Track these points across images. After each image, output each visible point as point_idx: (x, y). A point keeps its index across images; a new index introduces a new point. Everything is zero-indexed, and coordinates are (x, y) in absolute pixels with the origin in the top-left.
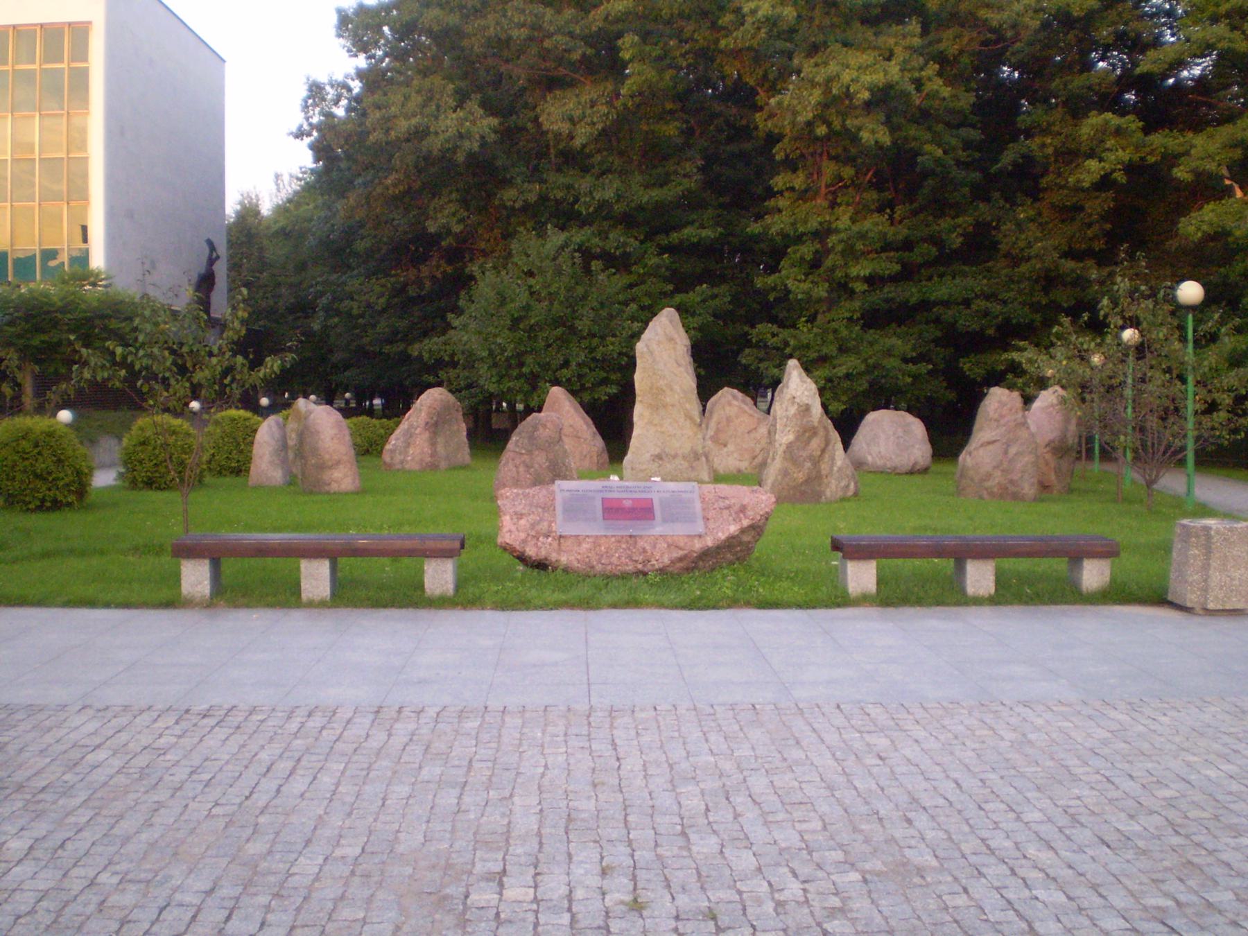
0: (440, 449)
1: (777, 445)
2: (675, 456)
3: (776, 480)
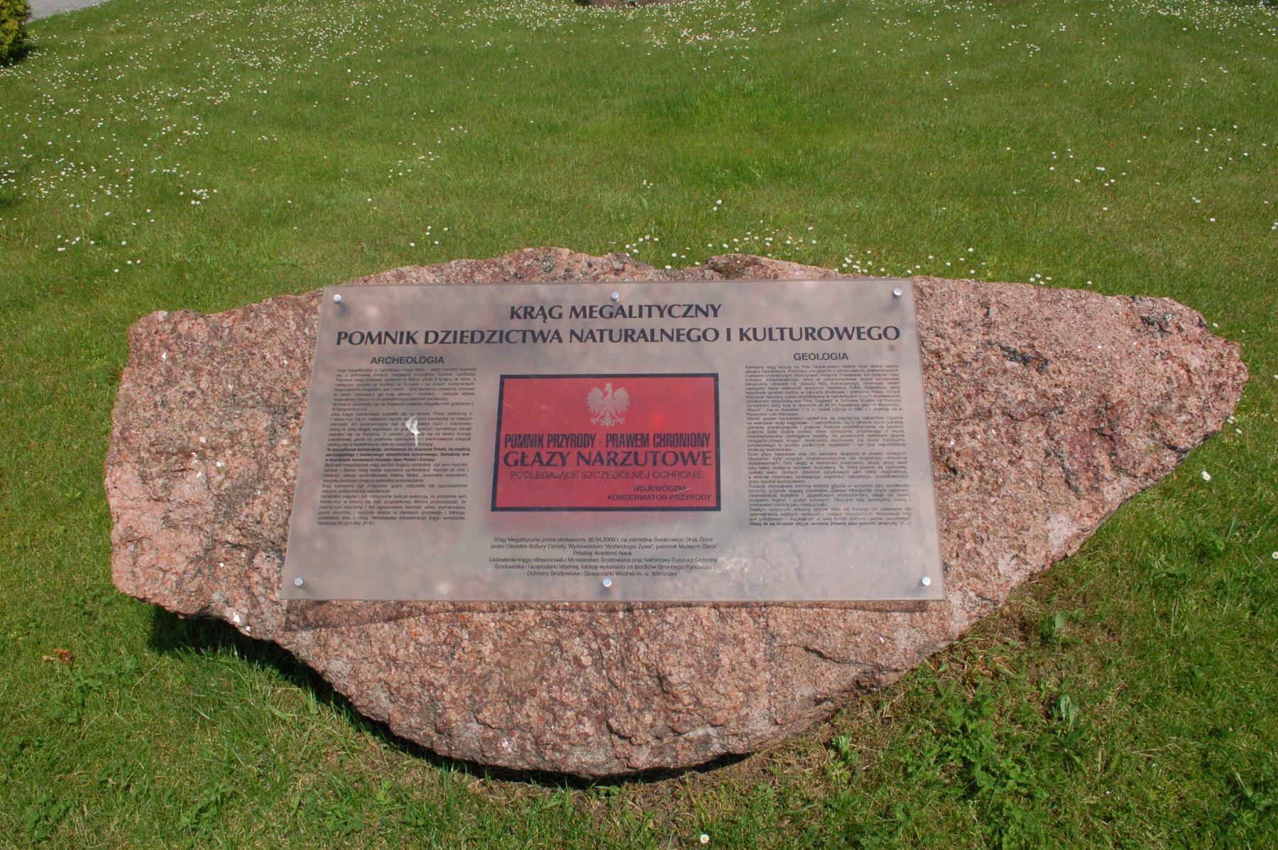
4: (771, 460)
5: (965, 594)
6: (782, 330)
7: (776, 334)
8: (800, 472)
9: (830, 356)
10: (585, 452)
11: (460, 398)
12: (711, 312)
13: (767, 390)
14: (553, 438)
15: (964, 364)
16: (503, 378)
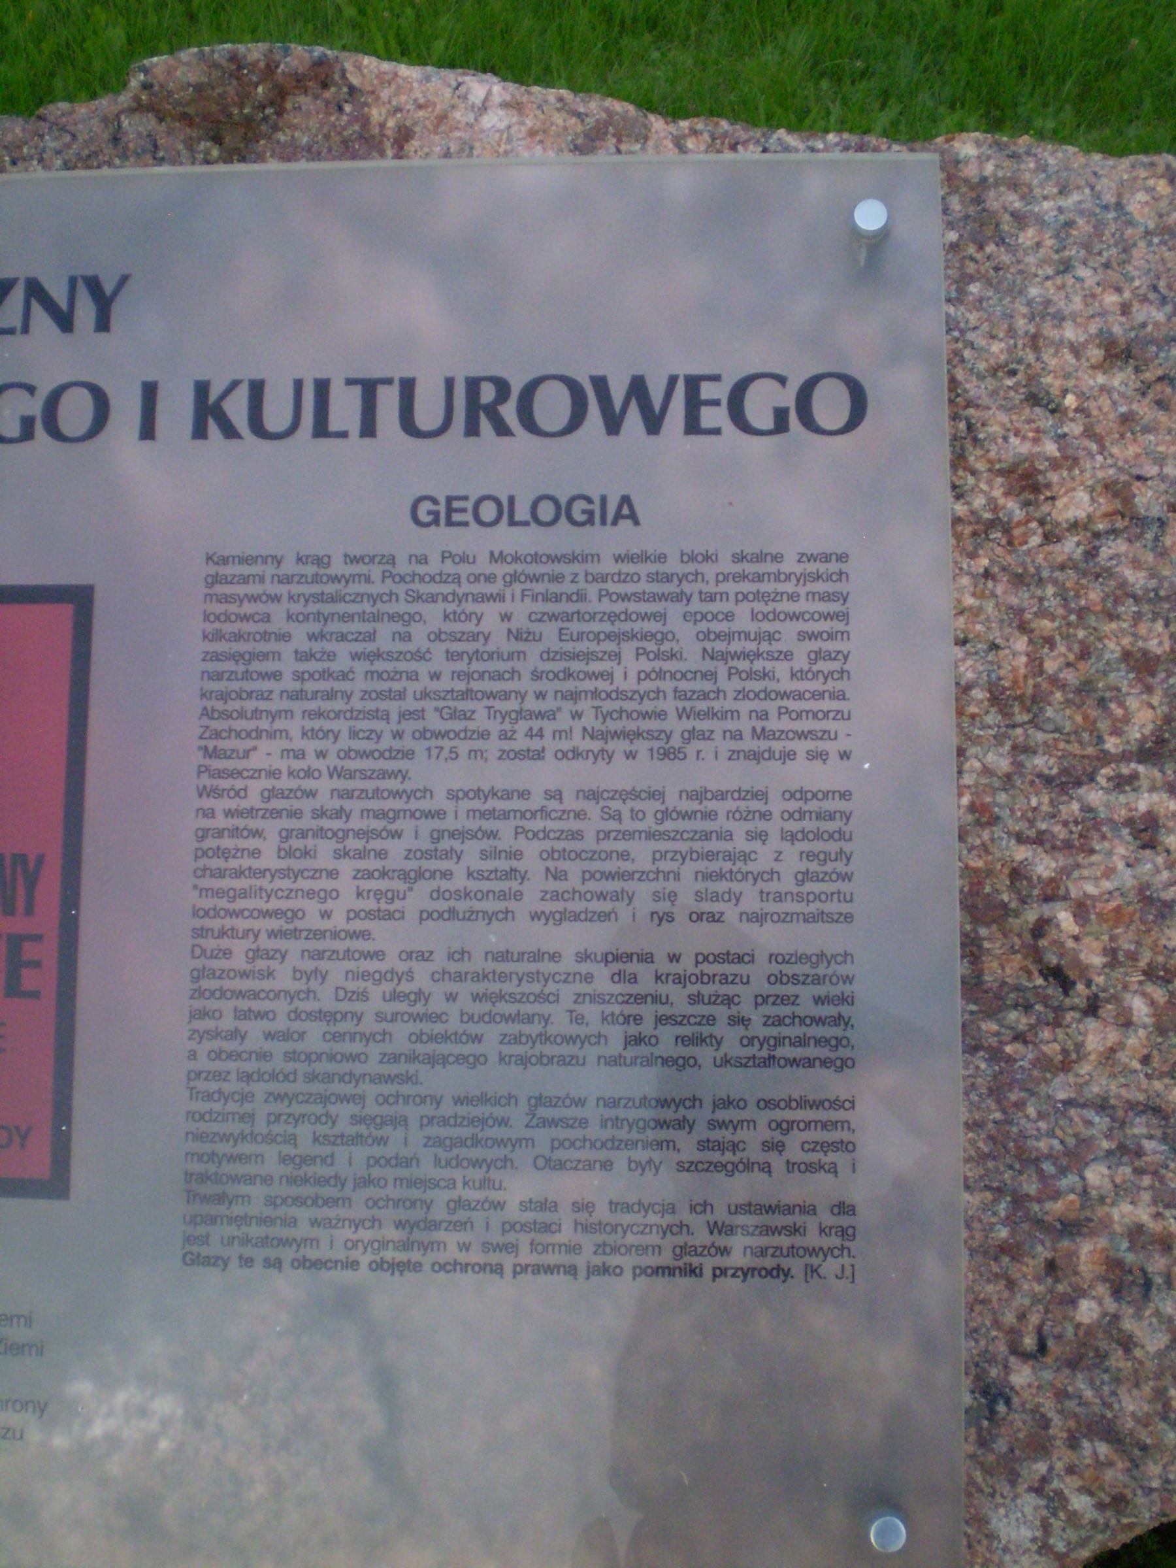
4: (284, 980)
5: (1058, 1501)
6: (369, 388)
7: (345, 409)
8: (402, 1031)
9: (563, 511)
12: (85, 312)
13: (288, 665)
15: (1129, 521)
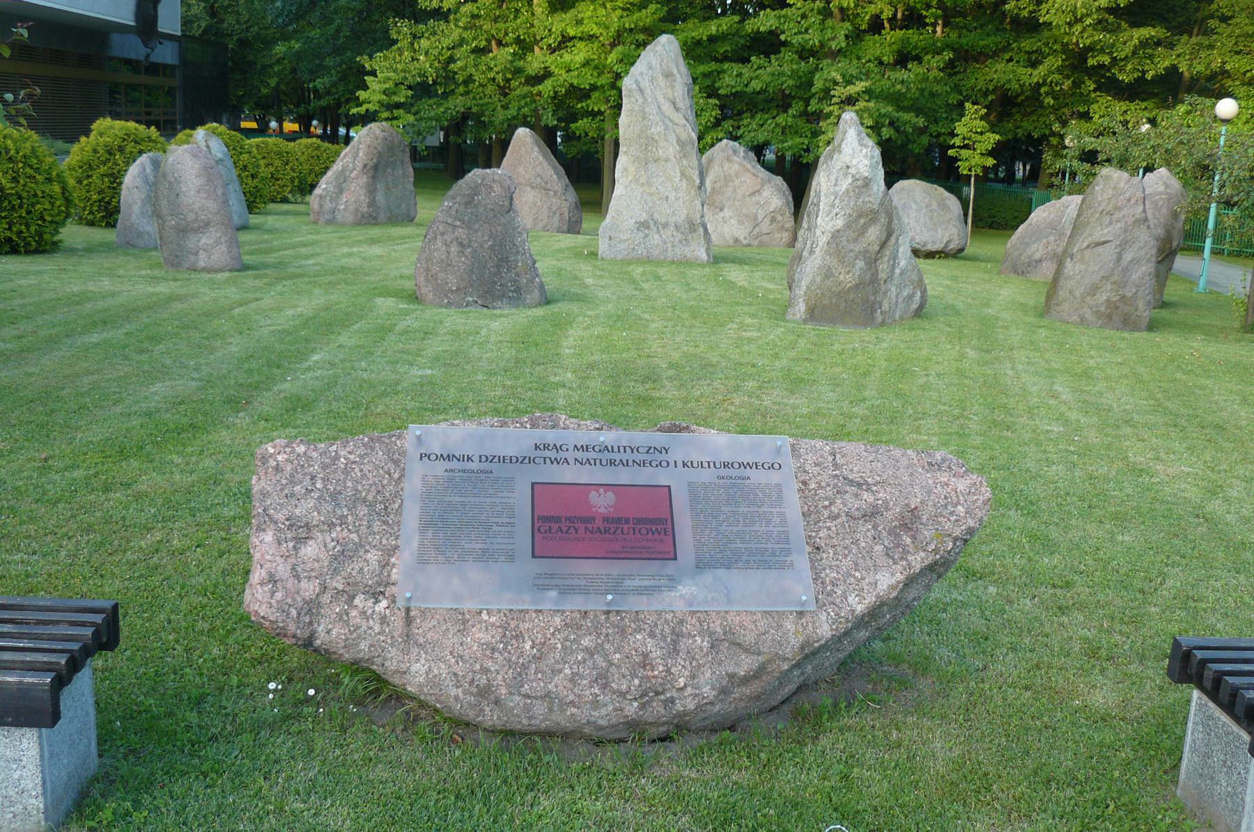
0: (380, 197)
1: (818, 232)
2: (665, 225)
3: (813, 281)
7: (705, 465)
10: (590, 526)
11: (506, 494)
14: (569, 519)
15: (820, 487)
16: (533, 484)
